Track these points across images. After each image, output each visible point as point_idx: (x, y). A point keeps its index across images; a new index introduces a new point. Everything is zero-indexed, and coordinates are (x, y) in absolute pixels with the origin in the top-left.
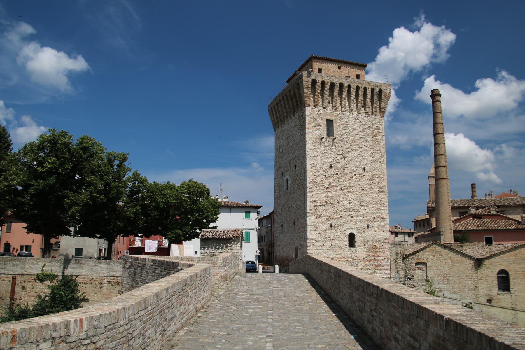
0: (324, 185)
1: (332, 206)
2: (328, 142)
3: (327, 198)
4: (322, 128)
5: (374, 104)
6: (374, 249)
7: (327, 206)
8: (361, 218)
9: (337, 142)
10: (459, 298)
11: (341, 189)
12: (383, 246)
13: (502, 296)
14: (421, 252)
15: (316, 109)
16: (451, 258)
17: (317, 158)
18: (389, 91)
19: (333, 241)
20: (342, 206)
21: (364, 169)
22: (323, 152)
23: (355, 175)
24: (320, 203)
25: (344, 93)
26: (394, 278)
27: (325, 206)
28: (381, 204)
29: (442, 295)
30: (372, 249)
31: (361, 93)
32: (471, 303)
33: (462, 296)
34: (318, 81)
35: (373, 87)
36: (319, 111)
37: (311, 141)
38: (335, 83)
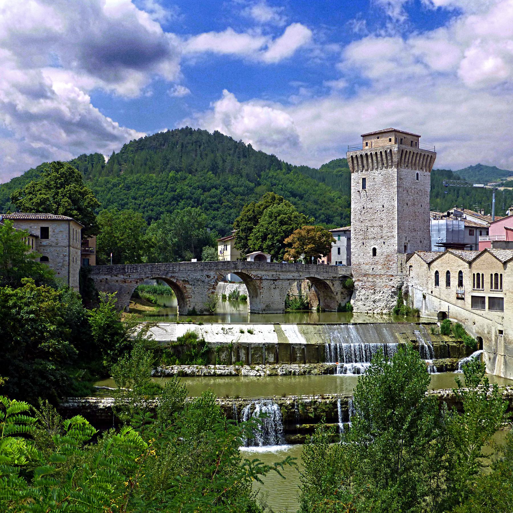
2: (363, 193)
21: (383, 206)
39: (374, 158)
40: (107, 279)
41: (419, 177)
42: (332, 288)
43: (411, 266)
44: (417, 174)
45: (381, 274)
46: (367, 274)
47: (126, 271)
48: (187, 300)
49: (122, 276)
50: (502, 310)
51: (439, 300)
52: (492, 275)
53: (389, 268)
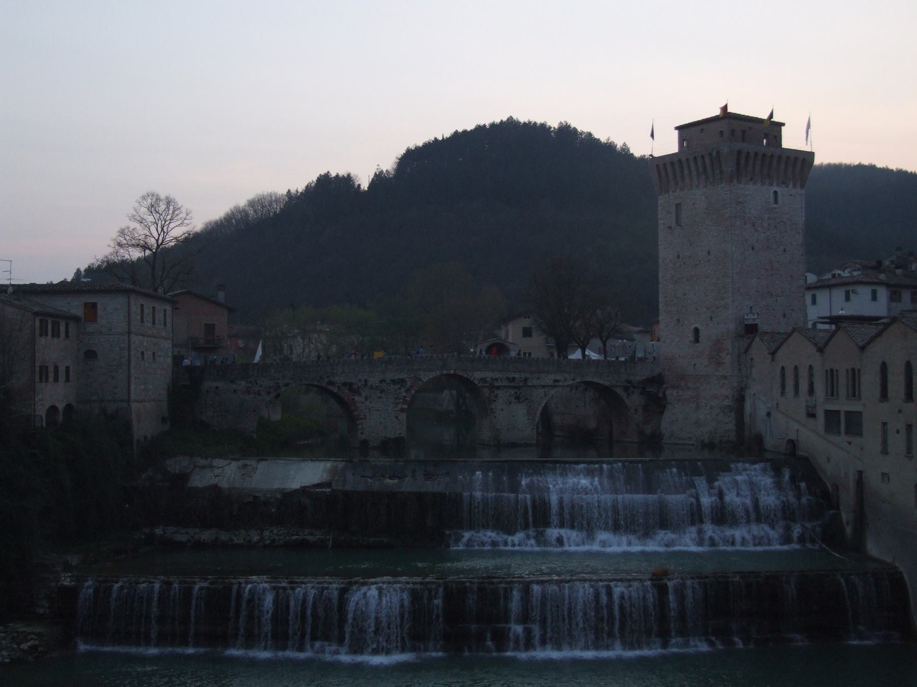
15: (667, 195)
21: (709, 252)
23: (700, 261)
28: (724, 291)
36: (669, 196)
39: (693, 168)
40: (217, 388)
41: (780, 198)
42: (627, 402)
43: (752, 359)
44: (775, 193)
47: (251, 373)
48: (358, 422)
49: (243, 383)
53: (719, 364)
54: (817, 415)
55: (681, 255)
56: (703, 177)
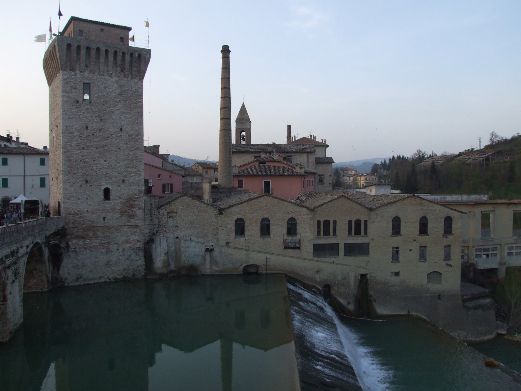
0: (79, 145)
1: (87, 164)
3: (82, 158)
4: (79, 91)
5: (133, 68)
6: (129, 202)
7: (83, 165)
8: (116, 174)
9: (94, 105)
10: (203, 241)
11: (97, 148)
12: (137, 198)
13: (237, 240)
14: (173, 203)
15: (73, 73)
16: (197, 209)
17: (73, 120)
18: (149, 56)
19: (88, 196)
20: (97, 164)
21: (121, 130)
22: (79, 114)
23: (112, 135)
24: (76, 162)
25: (101, 57)
26: (148, 226)
27: (81, 164)
28: (137, 161)
29: (189, 239)
30: (127, 202)
31: (119, 57)
32: (213, 246)
33: (205, 240)
34: (73, 46)
35: (132, 52)
36: (75, 74)
37: (67, 104)
38: (92, 48)
39: (111, 58)
45: (118, 226)
46: (94, 227)
50: (368, 254)
51: (244, 252)
52: (350, 222)
53: (131, 217)
54: (301, 248)
55: (89, 127)
56: (119, 69)
